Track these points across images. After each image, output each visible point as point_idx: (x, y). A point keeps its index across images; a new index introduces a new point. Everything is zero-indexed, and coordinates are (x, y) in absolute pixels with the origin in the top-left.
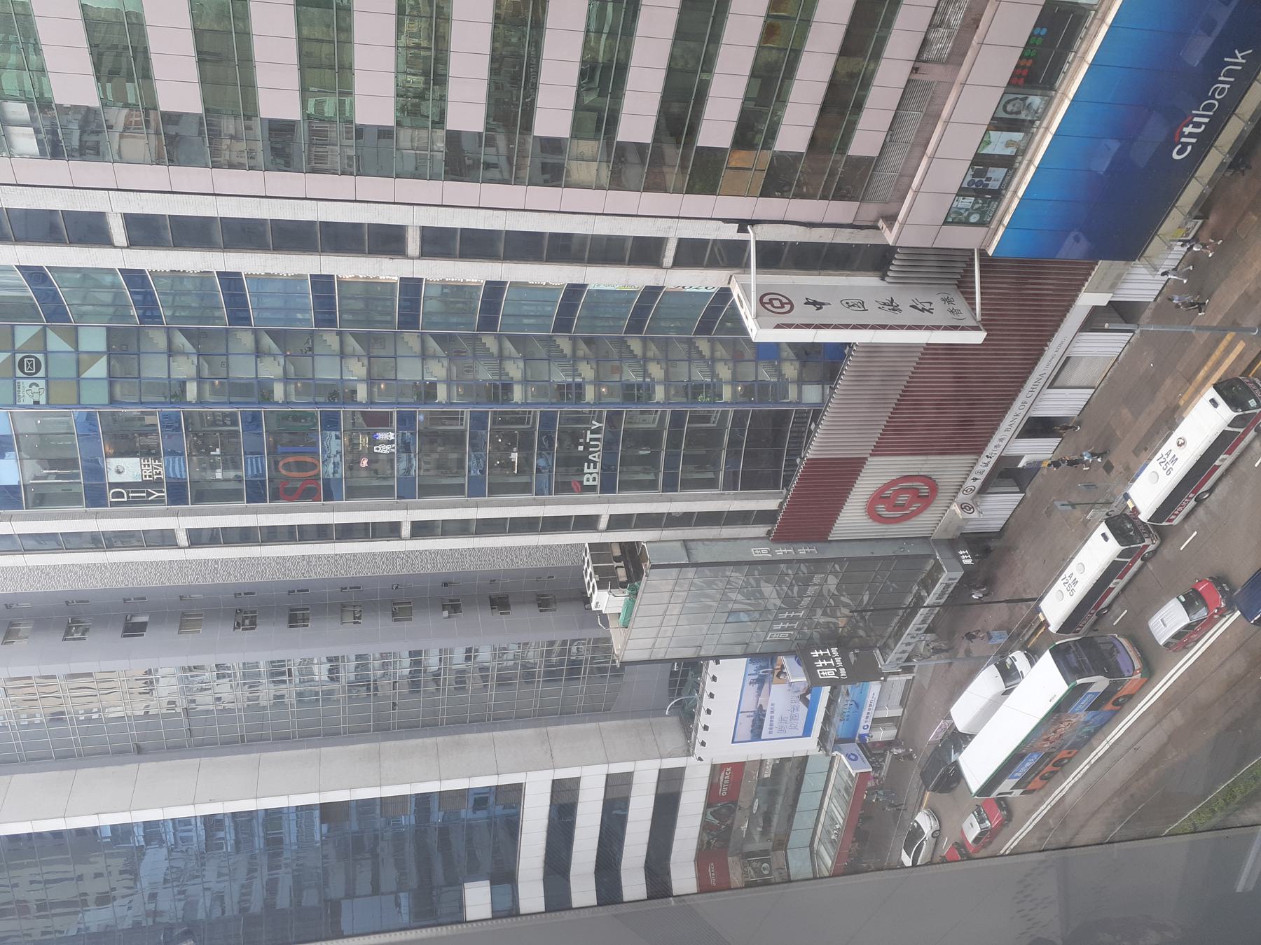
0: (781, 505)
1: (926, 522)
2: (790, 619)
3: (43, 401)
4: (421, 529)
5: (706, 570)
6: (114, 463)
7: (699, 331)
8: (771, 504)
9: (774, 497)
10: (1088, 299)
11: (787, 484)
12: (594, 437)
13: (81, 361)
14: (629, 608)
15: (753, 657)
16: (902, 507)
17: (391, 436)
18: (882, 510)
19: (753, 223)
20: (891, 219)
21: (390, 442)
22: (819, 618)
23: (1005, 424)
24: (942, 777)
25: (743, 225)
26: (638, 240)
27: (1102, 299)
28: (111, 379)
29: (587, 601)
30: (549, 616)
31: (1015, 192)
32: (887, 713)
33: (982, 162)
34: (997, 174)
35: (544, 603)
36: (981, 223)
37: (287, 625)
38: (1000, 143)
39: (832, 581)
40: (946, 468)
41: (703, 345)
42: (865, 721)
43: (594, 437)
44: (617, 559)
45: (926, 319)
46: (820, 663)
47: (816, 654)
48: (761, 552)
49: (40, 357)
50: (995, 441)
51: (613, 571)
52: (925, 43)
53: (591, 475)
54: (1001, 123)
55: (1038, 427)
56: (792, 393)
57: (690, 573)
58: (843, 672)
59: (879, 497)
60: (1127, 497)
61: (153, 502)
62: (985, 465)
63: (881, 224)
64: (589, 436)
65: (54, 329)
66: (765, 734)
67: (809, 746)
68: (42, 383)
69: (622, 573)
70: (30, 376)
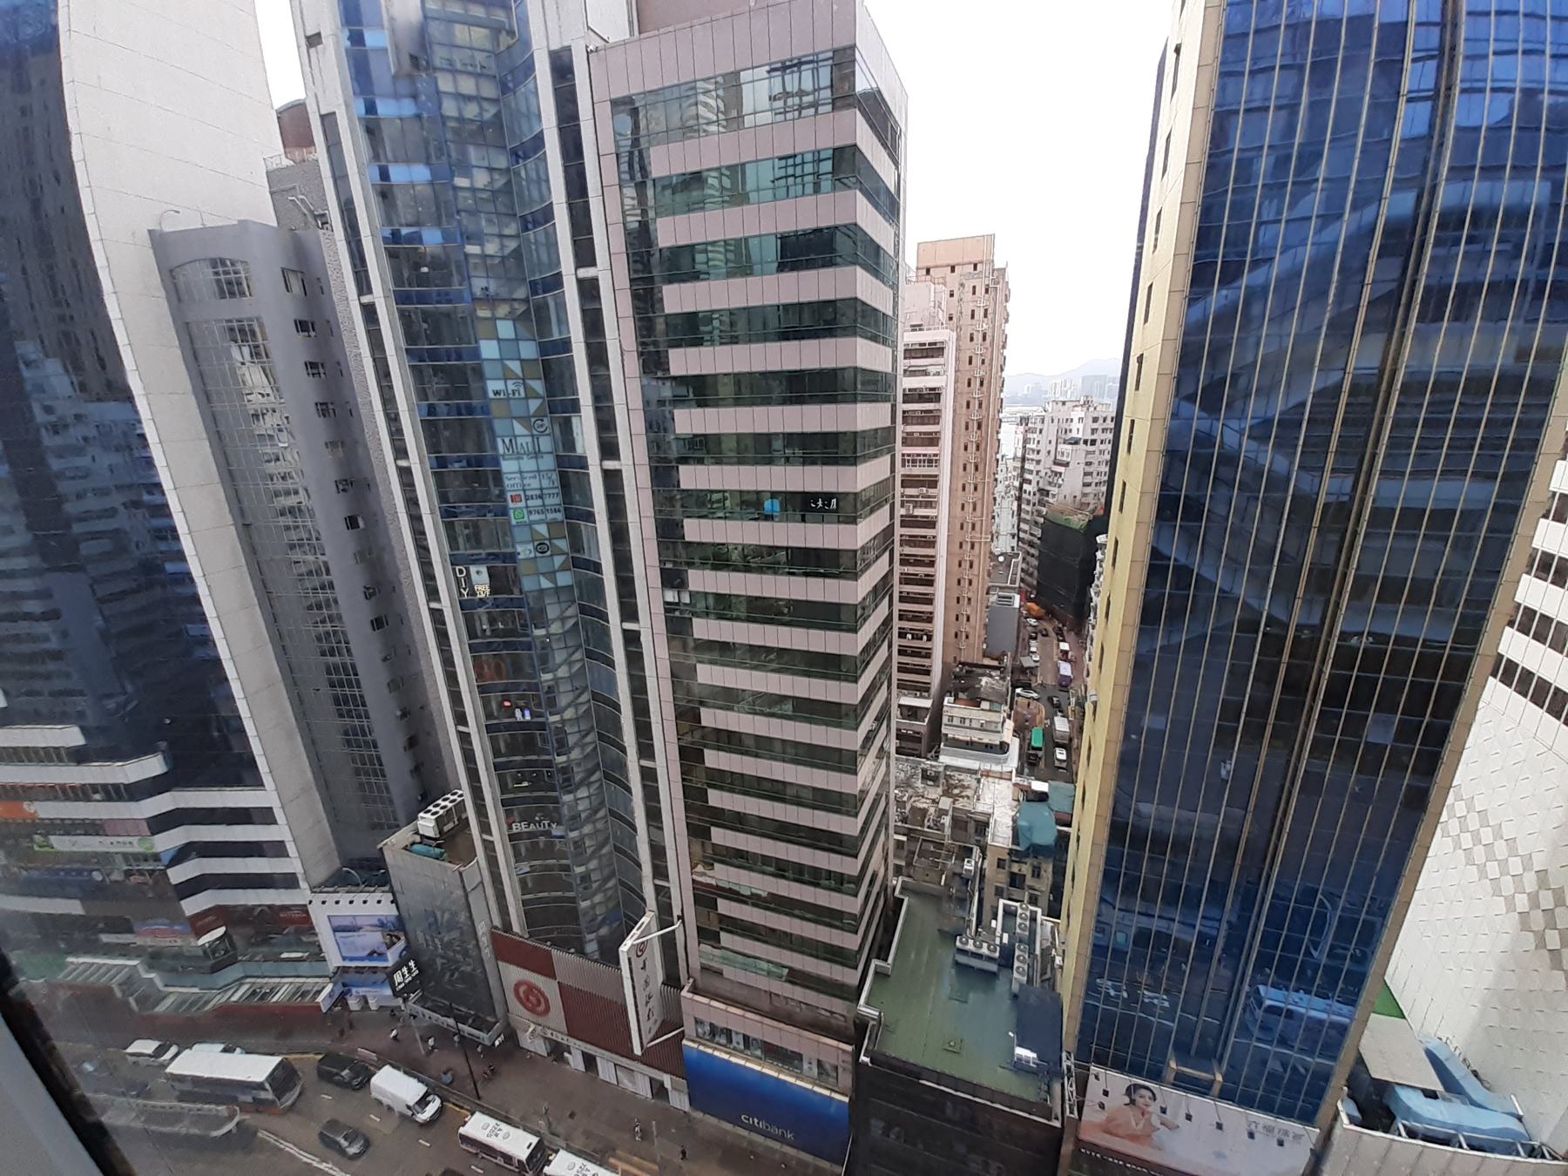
1: (518, 1012)
5: (463, 901)
6: (484, 569)
7: (616, 848)
8: (516, 928)
10: (667, 1080)
13: (551, 575)
15: (399, 918)
16: (528, 1000)
17: (528, 717)
18: (522, 989)
19: (683, 922)
20: (695, 990)
21: (523, 716)
22: (439, 961)
23: (589, 1046)
24: (330, 1072)
25: (681, 918)
26: (659, 810)
27: (668, 1085)
29: (424, 809)
30: (408, 777)
32: (371, 1002)
33: (728, 1033)
34: (723, 1041)
35: (417, 770)
36: (698, 1036)
37: (372, 618)
38: (738, 1040)
39: (469, 969)
40: (557, 1016)
42: (362, 991)
45: (643, 1018)
46: (405, 970)
47: (412, 964)
48: (482, 928)
50: (578, 1042)
52: (777, 995)
54: (746, 1038)
55: (590, 1061)
56: (590, 937)
57: (460, 892)
59: (531, 988)
60: (556, 1152)
62: (559, 1038)
65: (567, 559)
66: (338, 934)
67: (334, 960)
68: (532, 555)
70: (536, 549)
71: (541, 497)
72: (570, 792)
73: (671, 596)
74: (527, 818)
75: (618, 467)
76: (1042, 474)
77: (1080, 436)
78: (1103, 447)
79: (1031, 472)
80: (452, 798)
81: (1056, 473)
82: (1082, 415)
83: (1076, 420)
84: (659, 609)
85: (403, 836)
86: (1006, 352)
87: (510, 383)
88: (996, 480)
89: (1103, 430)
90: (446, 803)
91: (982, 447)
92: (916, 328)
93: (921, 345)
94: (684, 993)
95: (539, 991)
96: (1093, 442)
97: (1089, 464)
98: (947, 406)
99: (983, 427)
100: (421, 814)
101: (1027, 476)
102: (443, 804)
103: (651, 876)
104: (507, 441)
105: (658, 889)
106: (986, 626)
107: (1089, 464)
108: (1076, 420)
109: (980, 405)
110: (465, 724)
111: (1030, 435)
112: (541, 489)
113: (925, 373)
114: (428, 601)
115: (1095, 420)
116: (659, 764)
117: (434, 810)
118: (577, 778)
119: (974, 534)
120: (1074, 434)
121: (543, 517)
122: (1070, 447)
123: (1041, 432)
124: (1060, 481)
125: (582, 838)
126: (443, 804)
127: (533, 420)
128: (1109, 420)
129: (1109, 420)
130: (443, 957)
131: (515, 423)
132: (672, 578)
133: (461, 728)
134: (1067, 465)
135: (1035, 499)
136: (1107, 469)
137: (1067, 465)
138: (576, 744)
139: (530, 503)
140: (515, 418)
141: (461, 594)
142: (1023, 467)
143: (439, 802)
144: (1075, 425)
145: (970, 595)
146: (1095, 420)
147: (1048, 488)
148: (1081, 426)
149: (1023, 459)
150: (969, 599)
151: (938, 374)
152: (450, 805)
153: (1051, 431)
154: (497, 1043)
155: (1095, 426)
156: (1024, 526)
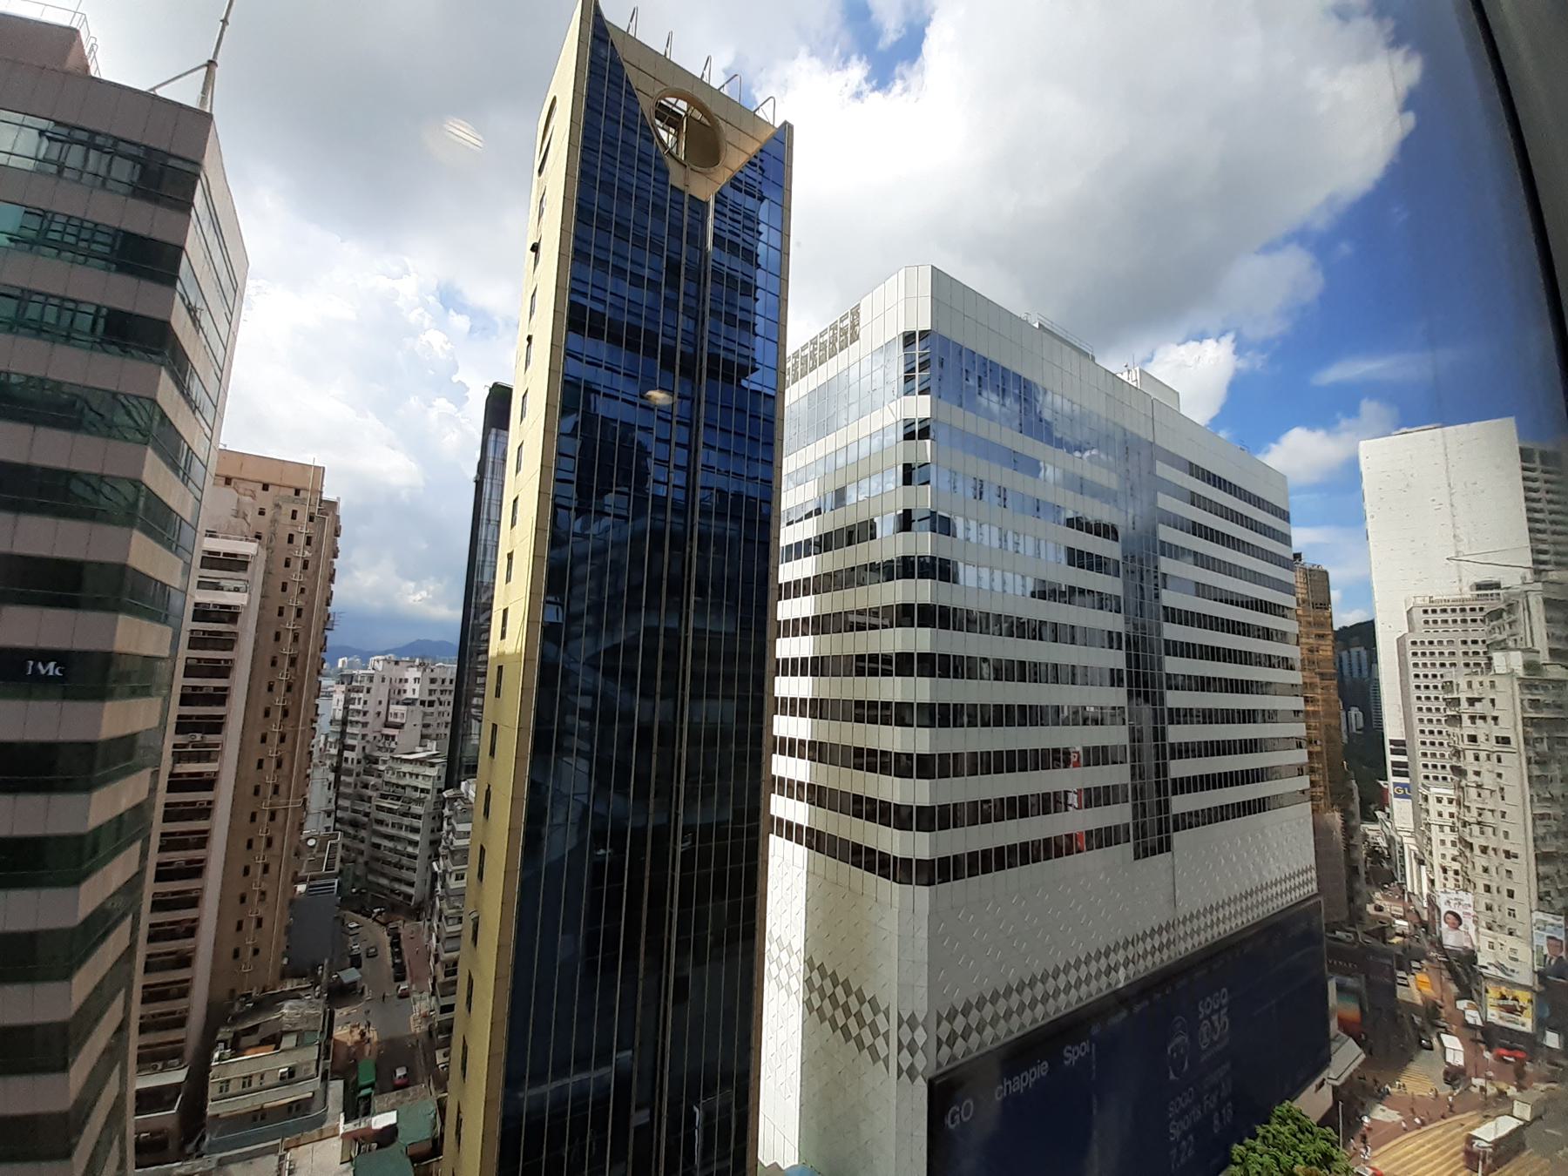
76: (370, 738)
77: (416, 696)
78: (441, 708)
79: (354, 736)
81: (387, 737)
82: (418, 675)
83: (411, 680)
86: (333, 587)
88: (314, 729)
89: (442, 692)
91: (295, 688)
92: (211, 534)
93: (227, 538)
96: (431, 704)
97: (426, 726)
98: (247, 630)
99: (299, 666)
101: (350, 742)
106: (288, 930)
107: (426, 726)
108: (411, 680)
109: (296, 638)
111: (353, 695)
113: (217, 587)
115: (433, 681)
119: (275, 799)
120: (409, 695)
122: (404, 708)
123: (368, 691)
124: (393, 745)
128: (447, 682)
129: (447, 682)
134: (400, 726)
135: (360, 768)
136: (448, 732)
137: (400, 726)
142: (343, 733)
144: (409, 686)
145: (264, 886)
146: (433, 681)
147: (377, 754)
148: (417, 686)
149: (344, 722)
150: (263, 893)
151: (237, 590)
153: (381, 691)
155: (433, 687)
156: (343, 803)
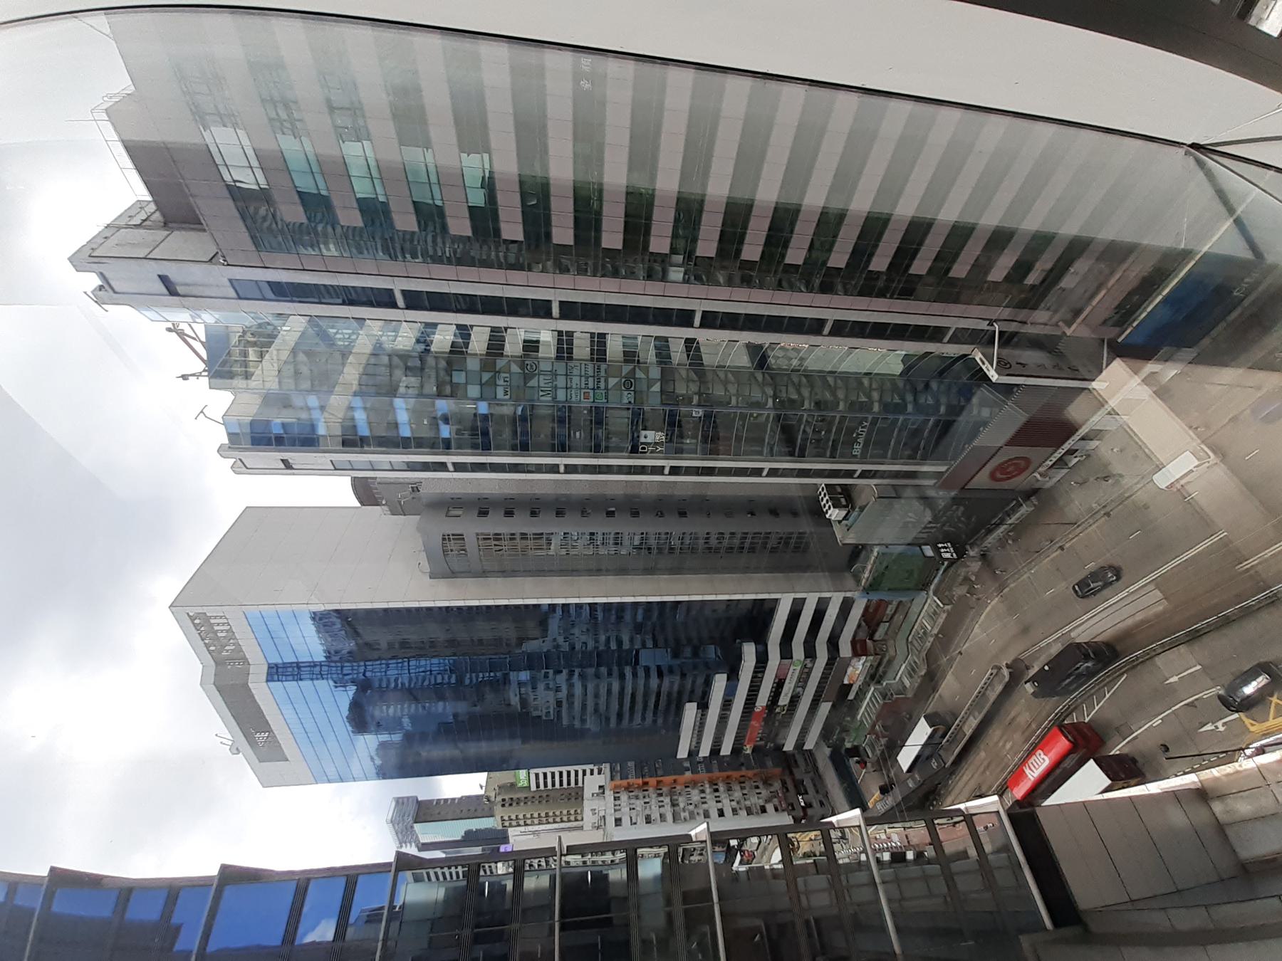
0: (947, 470)
2: (932, 528)
3: (633, 402)
4: (773, 473)
8: (943, 469)
9: (945, 465)
11: (954, 459)
12: (863, 431)
14: (845, 518)
18: (999, 476)
28: (662, 391)
31: (1145, 308)
39: (962, 508)
41: (934, 385)
43: (863, 431)
44: (840, 494)
46: (942, 550)
47: (940, 545)
49: (632, 380)
50: (1070, 441)
51: (839, 500)
53: (857, 450)
58: (954, 555)
59: (1001, 468)
61: (659, 452)
63: (1060, 324)
64: (860, 429)
68: (632, 393)
69: (843, 500)
70: (628, 389)
71: (587, 378)
72: (838, 404)
73: (676, 274)
74: (851, 443)
75: (557, 304)
80: (822, 495)
84: (684, 290)
85: (838, 531)
87: (498, 382)
90: (825, 500)
94: (1069, 332)
95: (1006, 462)
100: (827, 516)
102: (825, 501)
103: (939, 345)
104: (541, 393)
105: (955, 340)
110: (761, 470)
112: (581, 376)
114: (663, 474)
116: (831, 316)
117: (827, 507)
118: (828, 396)
121: (602, 380)
125: (880, 401)
126: (825, 501)
127: (526, 371)
130: (944, 525)
131: (528, 385)
132: (656, 269)
133: (765, 473)
138: (799, 393)
139: (591, 385)
140: (525, 383)
141: (659, 452)
143: (822, 504)
152: (827, 497)
154: (1036, 503)
